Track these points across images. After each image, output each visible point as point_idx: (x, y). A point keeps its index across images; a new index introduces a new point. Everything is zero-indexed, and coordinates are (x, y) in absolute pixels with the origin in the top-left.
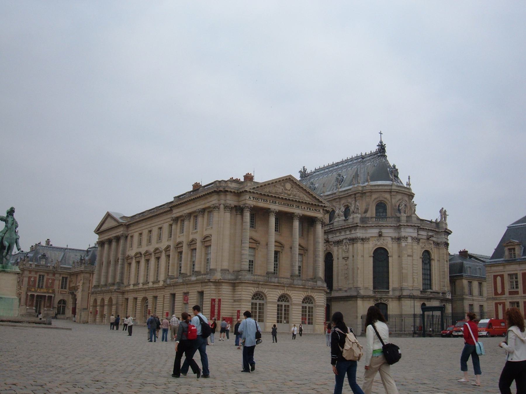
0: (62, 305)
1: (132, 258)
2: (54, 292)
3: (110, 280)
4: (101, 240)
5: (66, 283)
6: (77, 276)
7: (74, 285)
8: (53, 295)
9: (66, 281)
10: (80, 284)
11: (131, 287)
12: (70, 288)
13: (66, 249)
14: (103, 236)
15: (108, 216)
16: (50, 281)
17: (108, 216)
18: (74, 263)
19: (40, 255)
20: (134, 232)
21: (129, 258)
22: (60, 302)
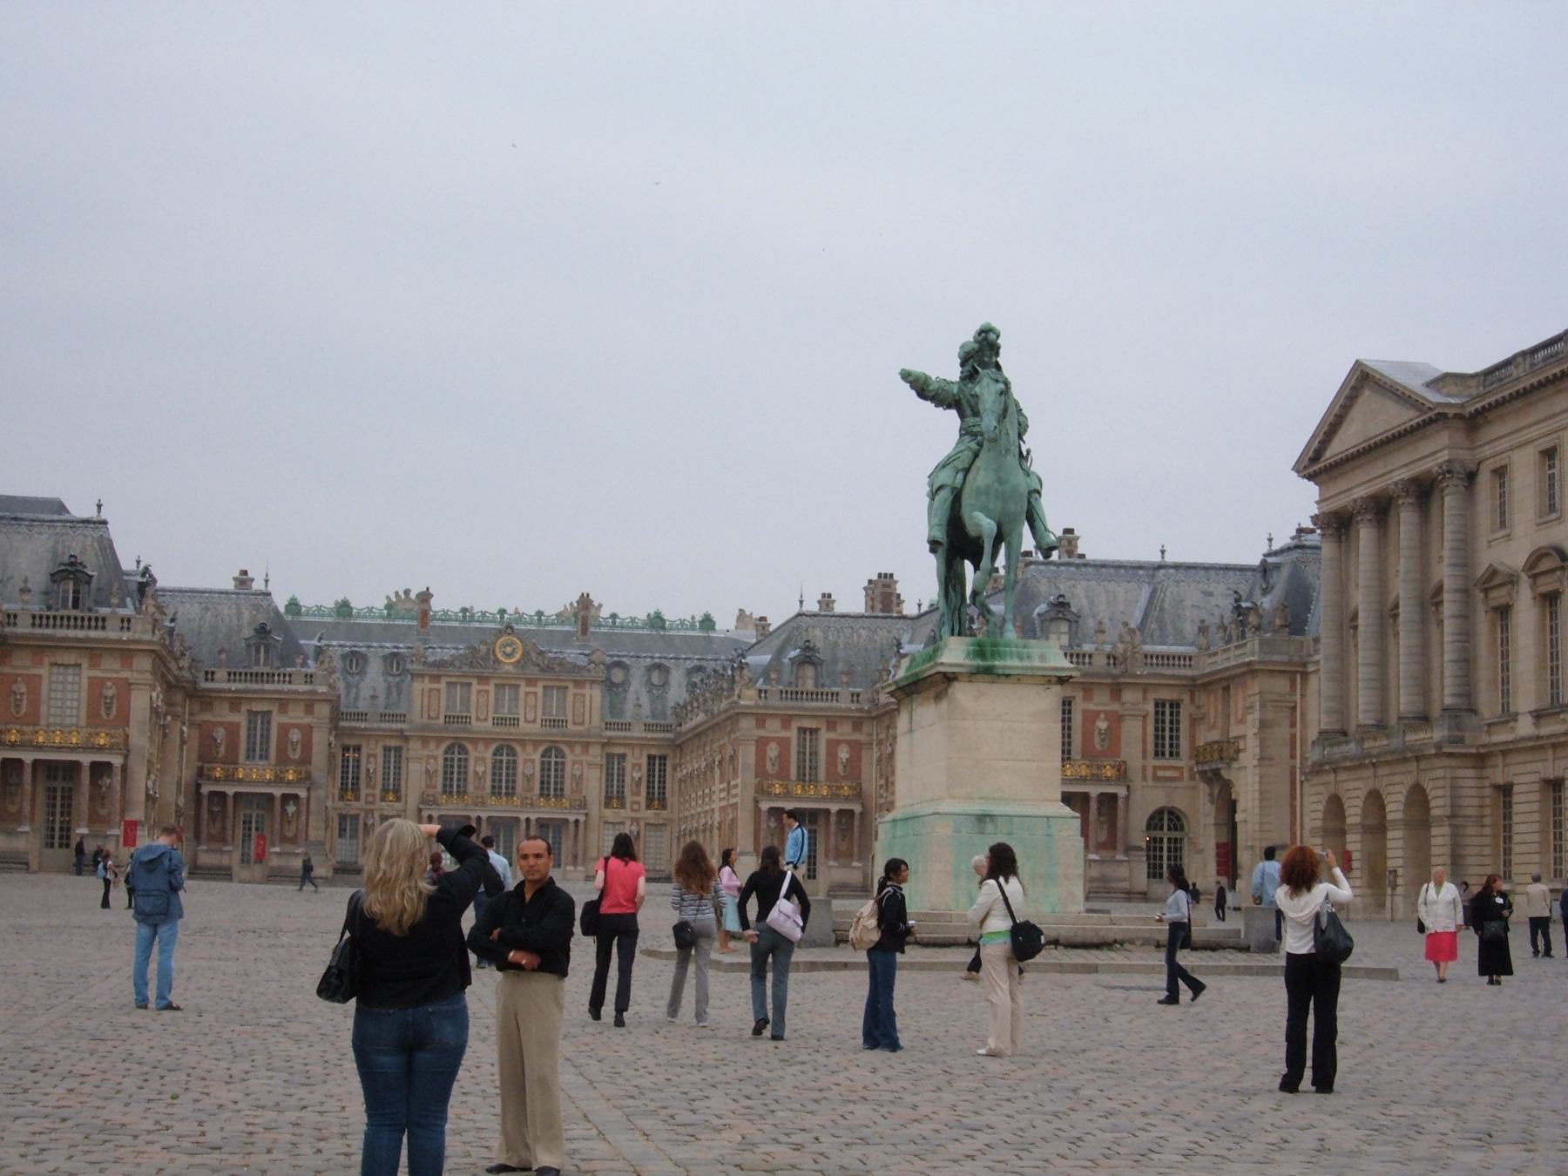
0: (1165, 834)
1: (1512, 581)
2: (1122, 774)
3: (1404, 700)
4: (1334, 505)
5: (1175, 729)
6: (1226, 689)
7: (1215, 735)
8: (1121, 791)
9: (1175, 722)
10: (1247, 730)
11: (1525, 727)
12: (1196, 754)
13: (1160, 567)
14: (1342, 484)
15: (1363, 380)
16: (1102, 725)
17: (1363, 380)
18: (1203, 629)
19: (1043, 608)
20: (1514, 446)
21: (1493, 579)
22: (1155, 821)
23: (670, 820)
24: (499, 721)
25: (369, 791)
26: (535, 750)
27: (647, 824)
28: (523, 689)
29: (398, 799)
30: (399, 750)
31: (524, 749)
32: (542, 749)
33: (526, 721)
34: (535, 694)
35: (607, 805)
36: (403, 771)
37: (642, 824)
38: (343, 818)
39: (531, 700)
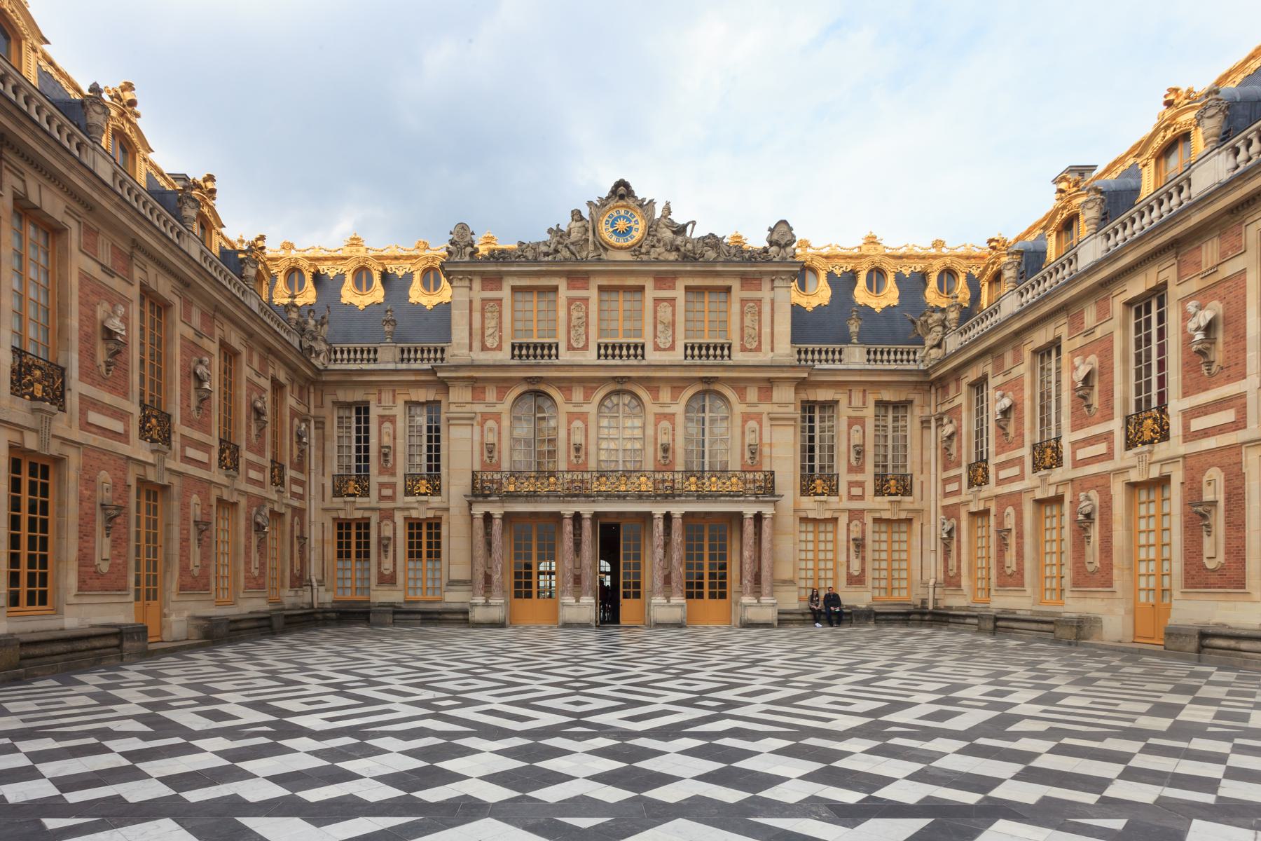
23: (919, 511)
24: (607, 350)
25: (385, 479)
26: (675, 398)
27: (876, 520)
28: (651, 293)
29: (436, 491)
30: (433, 406)
31: (656, 398)
32: (688, 393)
33: (657, 348)
34: (672, 301)
35: (806, 490)
36: (443, 443)
37: (868, 519)
38: (343, 526)
39: (665, 312)
